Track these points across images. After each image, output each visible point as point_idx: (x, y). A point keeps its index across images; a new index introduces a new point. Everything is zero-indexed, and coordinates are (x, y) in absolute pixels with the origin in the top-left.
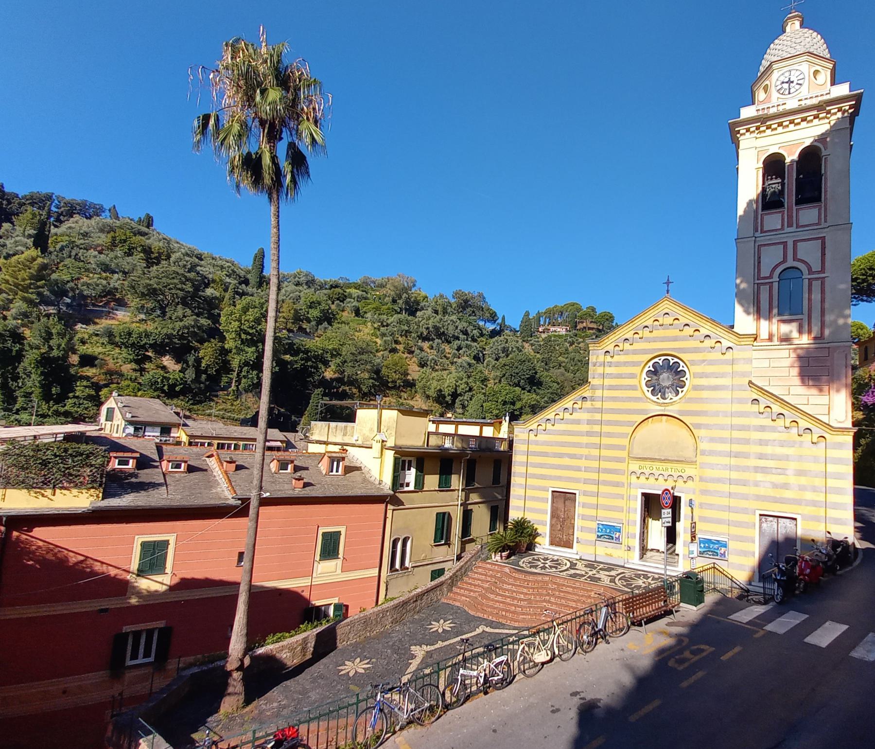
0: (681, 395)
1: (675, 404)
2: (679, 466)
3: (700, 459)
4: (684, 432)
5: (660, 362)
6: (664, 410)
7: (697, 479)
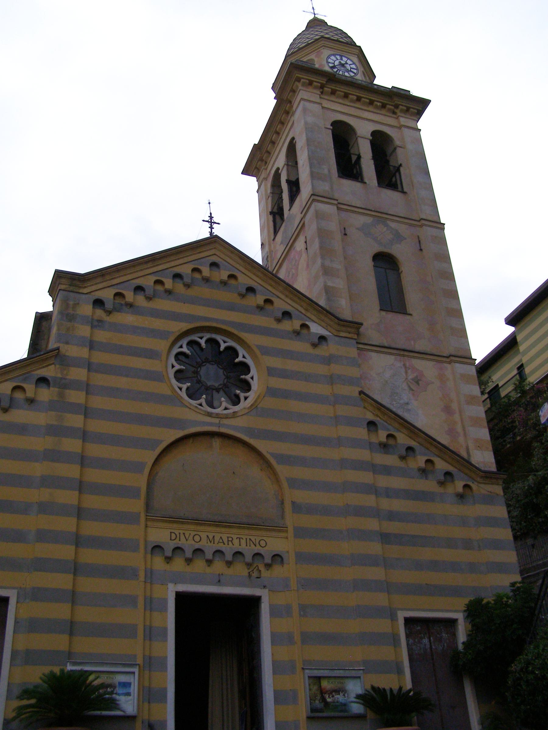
0: (243, 404)
1: (233, 416)
4: (255, 471)
6: (219, 425)
7: (291, 559)
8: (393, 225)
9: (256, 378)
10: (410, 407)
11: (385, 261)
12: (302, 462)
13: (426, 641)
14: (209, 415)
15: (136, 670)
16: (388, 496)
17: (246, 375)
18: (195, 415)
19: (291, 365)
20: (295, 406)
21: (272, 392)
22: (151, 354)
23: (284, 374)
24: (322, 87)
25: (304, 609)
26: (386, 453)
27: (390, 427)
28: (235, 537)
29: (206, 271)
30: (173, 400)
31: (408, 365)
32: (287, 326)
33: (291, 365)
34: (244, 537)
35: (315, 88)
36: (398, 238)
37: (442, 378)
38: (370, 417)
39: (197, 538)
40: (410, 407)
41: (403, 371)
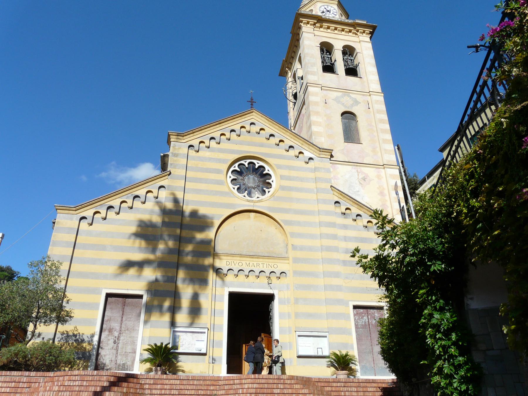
0: (267, 195)
2: (271, 262)
3: (291, 254)
5: (246, 164)
7: (290, 274)
8: (353, 96)
9: (274, 180)
10: (359, 193)
11: (348, 116)
12: (298, 224)
13: (365, 318)
14: (248, 201)
15: (206, 330)
16: (346, 241)
17: (269, 179)
18: (242, 201)
19: (293, 174)
20: (295, 195)
21: (283, 188)
22: (218, 171)
23: (289, 178)
24: (315, 24)
25: (297, 301)
26: (345, 218)
27: (348, 204)
28: (260, 263)
29: (248, 127)
30: (229, 194)
31: (359, 171)
32: (292, 153)
33: (293, 174)
34: (266, 263)
35: (311, 25)
36: (356, 102)
37: (379, 177)
38: (337, 199)
39: (240, 264)
40: (359, 193)
41: (357, 173)
